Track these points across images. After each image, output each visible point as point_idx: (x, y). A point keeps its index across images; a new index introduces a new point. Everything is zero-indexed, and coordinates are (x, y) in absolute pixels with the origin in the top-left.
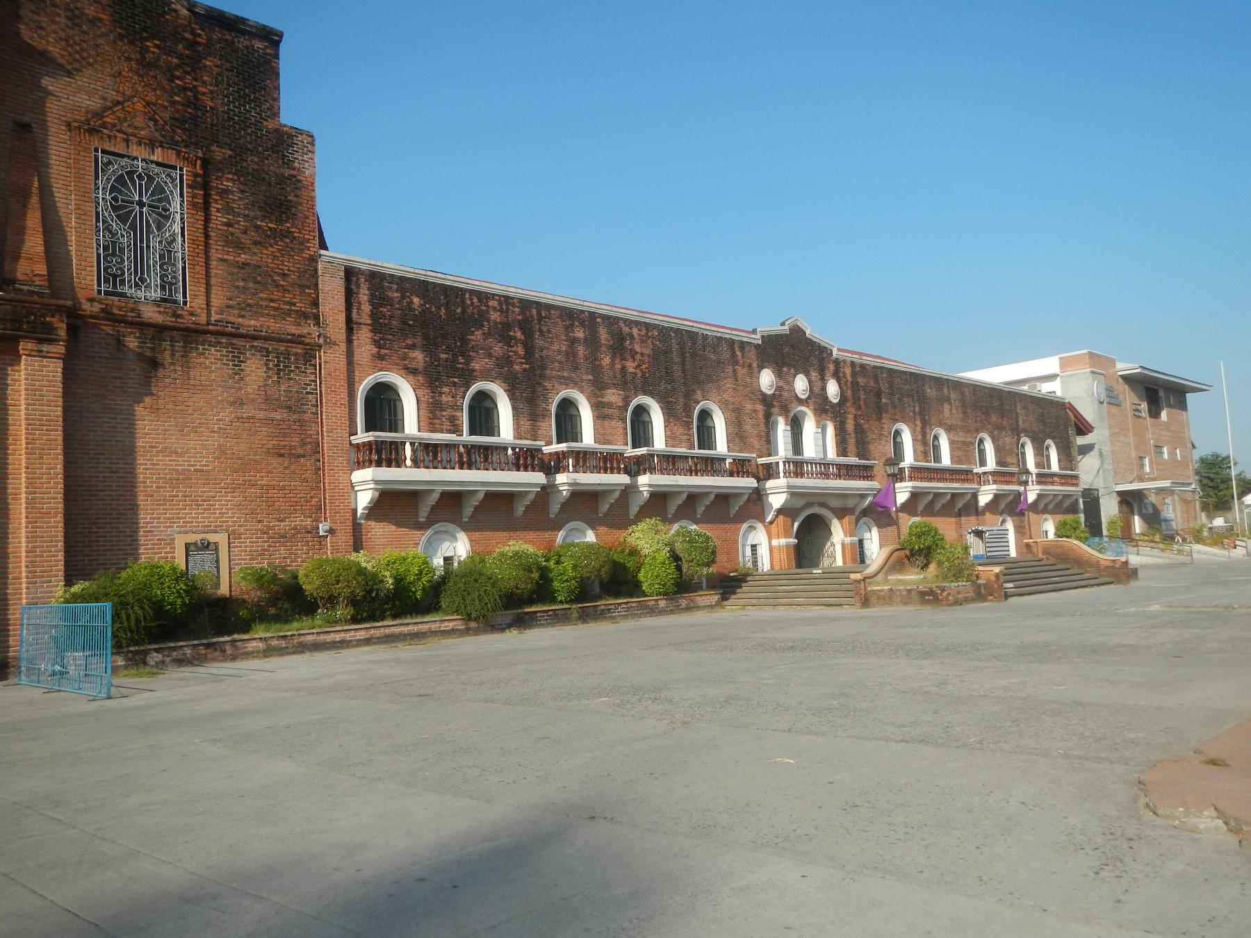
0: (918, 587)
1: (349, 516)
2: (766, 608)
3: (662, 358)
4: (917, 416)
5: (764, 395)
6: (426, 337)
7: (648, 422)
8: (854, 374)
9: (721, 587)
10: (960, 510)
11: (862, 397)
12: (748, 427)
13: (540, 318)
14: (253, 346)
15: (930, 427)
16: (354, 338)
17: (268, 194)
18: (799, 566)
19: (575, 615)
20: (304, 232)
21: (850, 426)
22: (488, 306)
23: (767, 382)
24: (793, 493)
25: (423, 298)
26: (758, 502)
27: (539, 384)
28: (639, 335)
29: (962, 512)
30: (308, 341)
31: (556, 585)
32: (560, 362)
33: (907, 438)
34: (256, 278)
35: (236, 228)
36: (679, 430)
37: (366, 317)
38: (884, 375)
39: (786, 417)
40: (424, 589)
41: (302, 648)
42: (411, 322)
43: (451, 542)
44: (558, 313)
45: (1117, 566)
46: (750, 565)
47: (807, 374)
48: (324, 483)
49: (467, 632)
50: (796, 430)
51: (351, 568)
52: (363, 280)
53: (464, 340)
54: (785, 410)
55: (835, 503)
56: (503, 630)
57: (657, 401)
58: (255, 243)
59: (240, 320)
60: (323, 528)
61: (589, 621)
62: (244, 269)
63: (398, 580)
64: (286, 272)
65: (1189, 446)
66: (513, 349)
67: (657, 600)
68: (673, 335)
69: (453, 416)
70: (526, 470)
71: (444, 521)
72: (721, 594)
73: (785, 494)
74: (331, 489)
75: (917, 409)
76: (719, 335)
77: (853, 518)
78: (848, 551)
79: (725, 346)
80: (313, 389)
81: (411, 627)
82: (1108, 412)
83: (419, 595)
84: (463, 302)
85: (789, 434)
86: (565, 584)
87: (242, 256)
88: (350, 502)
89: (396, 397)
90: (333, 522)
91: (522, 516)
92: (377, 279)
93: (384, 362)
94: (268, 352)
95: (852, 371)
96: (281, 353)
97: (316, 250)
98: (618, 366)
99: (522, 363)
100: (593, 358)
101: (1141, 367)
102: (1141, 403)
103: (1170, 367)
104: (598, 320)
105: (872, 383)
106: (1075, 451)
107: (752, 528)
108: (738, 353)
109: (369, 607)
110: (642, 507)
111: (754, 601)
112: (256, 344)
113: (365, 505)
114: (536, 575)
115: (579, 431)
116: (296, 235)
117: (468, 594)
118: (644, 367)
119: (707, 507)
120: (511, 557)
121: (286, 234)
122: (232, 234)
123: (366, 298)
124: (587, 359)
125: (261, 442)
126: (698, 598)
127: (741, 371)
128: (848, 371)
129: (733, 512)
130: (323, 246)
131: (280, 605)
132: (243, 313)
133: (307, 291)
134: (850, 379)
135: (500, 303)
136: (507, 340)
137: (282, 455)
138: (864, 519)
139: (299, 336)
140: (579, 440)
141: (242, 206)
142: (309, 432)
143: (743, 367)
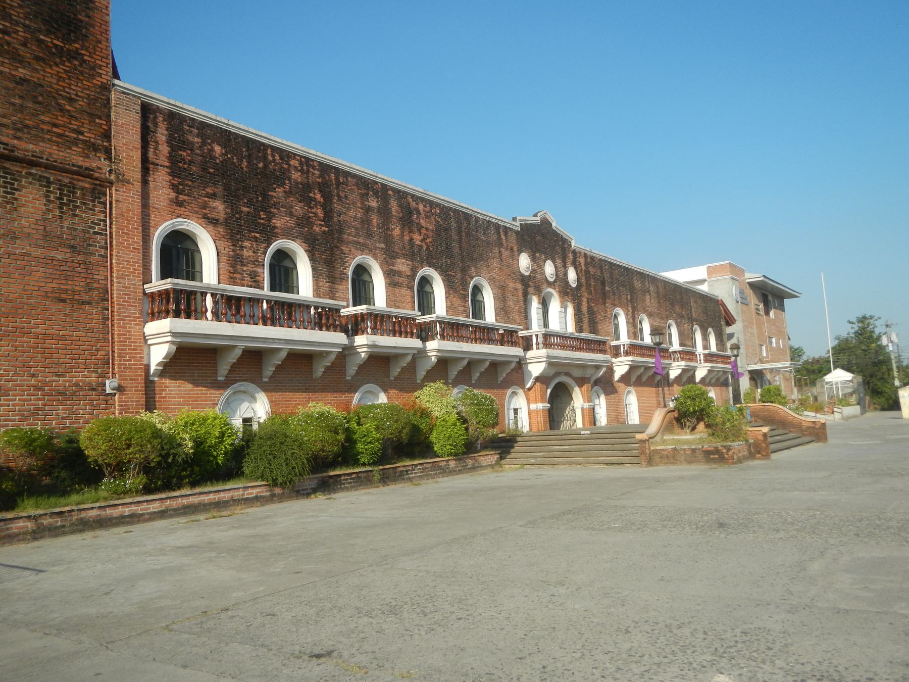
0: (703, 447)
1: (141, 372)
2: (545, 467)
3: (443, 234)
4: (629, 303)
5: (522, 275)
6: (227, 188)
7: (430, 293)
8: (586, 264)
9: (500, 447)
10: (658, 382)
12: (510, 303)
13: (338, 184)
14: (30, 174)
16: (150, 179)
17: (54, 7)
19: (377, 477)
20: (95, 57)
21: (584, 308)
22: (289, 165)
23: (525, 265)
24: (551, 363)
25: (225, 148)
27: (336, 247)
28: (424, 210)
30: (97, 175)
31: (360, 446)
32: (356, 229)
33: (622, 321)
34: (36, 97)
35: (13, 38)
36: (458, 302)
37: (164, 159)
38: (607, 267)
39: (539, 296)
40: (226, 453)
41: (85, 526)
42: (211, 171)
43: (250, 402)
44: (354, 180)
45: (817, 427)
47: (554, 262)
48: (112, 334)
49: (272, 499)
51: (145, 430)
52: (161, 119)
53: (265, 196)
54: (538, 290)
55: (577, 373)
56: (308, 495)
57: (439, 273)
58: (38, 59)
59: (16, 141)
60: (110, 385)
61: (389, 483)
62: (22, 85)
63: (199, 443)
64: (73, 96)
66: (313, 210)
67: (447, 461)
68: (452, 214)
69: (255, 272)
70: (328, 330)
71: (244, 381)
72: (499, 454)
74: (120, 342)
75: (629, 297)
77: (590, 385)
78: (587, 414)
79: (492, 230)
80: (102, 229)
81: (211, 496)
82: (742, 309)
83: (220, 459)
84: (265, 157)
86: (369, 446)
87: (20, 70)
88: (142, 357)
89: (192, 247)
90: (122, 378)
91: (321, 377)
92: (175, 120)
93: (182, 209)
94: (49, 183)
96: (64, 186)
97: (109, 78)
98: (407, 238)
99: (321, 225)
100: (385, 227)
101: (764, 276)
102: (760, 304)
103: (782, 278)
104: (390, 192)
106: (725, 337)
107: (514, 393)
108: (503, 237)
109: (163, 474)
110: (429, 372)
111: (533, 461)
112: (34, 171)
113: (160, 360)
114: (341, 437)
115: (372, 296)
116: (86, 58)
117: (274, 458)
118: (428, 240)
119: (482, 373)
120: (317, 418)
121: (74, 55)
122: (8, 43)
123: (164, 138)
124: (380, 228)
125: (36, 284)
126: (481, 458)
127: (506, 253)
128: (582, 261)
129: (501, 379)
130: (116, 76)
131: (57, 474)
132: (19, 134)
133: (97, 121)
134: (584, 269)
135: (301, 163)
136: (308, 201)
137: (63, 301)
138: (596, 388)
139: (87, 169)
140: (372, 303)
141: (22, 15)
142: (95, 277)
143: (507, 250)
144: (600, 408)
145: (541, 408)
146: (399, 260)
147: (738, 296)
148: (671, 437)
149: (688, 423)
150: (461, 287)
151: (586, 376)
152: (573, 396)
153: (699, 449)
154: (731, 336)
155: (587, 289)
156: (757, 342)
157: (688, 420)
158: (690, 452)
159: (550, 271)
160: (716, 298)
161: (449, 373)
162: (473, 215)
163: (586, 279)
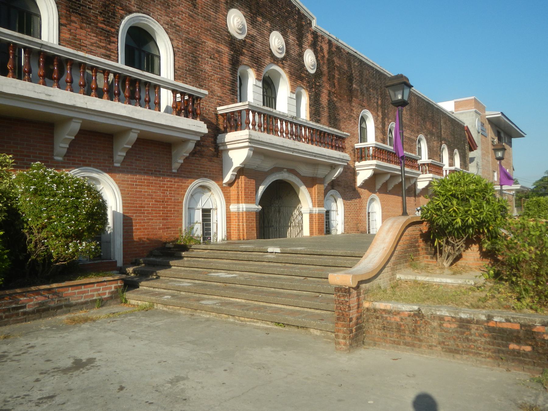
0: (490, 318)
4: (379, 108)
8: (330, 52)
11: (337, 76)
21: (324, 100)
26: (215, 159)
33: (371, 125)
38: (356, 64)
39: (258, 71)
46: (198, 230)
50: (269, 94)
54: (257, 64)
55: (305, 171)
65: (512, 168)
73: (247, 149)
75: (379, 102)
77: (323, 187)
78: (316, 220)
82: (481, 140)
85: (261, 91)
95: (329, 49)
101: (502, 113)
105: (346, 67)
107: (205, 188)
119: (129, 153)
126: (70, 291)
128: (326, 47)
134: (327, 56)
138: (332, 192)
144: (338, 214)
145: (245, 209)
147: (480, 128)
148: (411, 277)
149: (447, 249)
150: (100, 18)
152: (300, 197)
153: (478, 322)
154: (472, 160)
155: (329, 80)
156: (491, 169)
157: (448, 243)
158: (454, 326)
159: (276, 44)
160: (462, 124)
163: (328, 68)
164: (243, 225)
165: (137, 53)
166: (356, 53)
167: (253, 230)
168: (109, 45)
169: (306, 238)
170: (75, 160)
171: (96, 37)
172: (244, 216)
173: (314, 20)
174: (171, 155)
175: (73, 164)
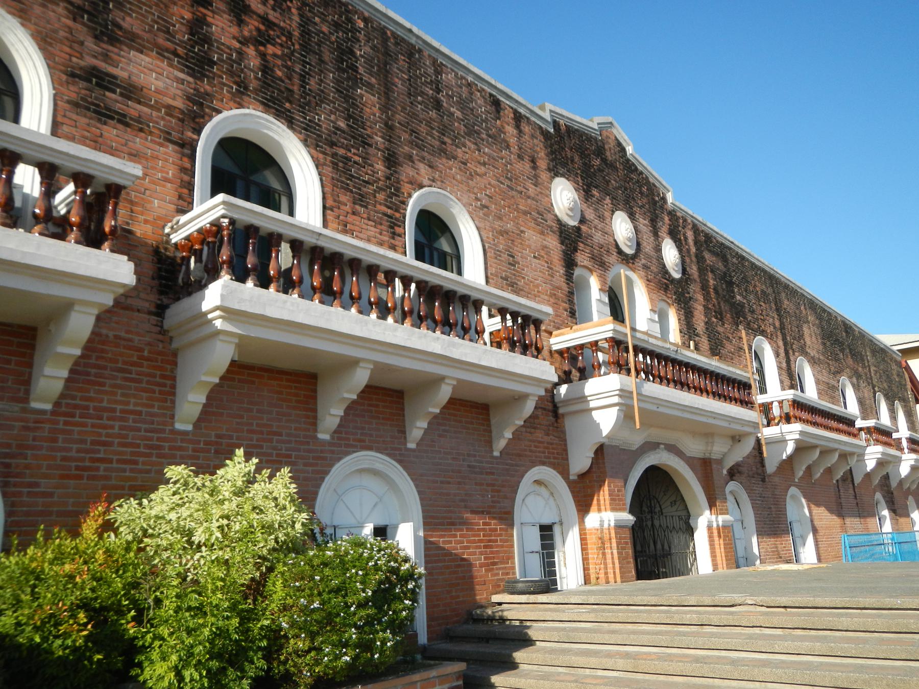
5: (559, 221)
10: (837, 481)
15: (794, 354)
18: (644, 573)
29: (840, 483)
47: (632, 216)
54: (601, 265)
55: (695, 447)
76: (470, 79)
95: (695, 237)
105: (720, 265)
118: (270, 49)
119: (436, 422)
128: (690, 234)
129: (500, 444)
134: (693, 250)
145: (612, 524)
146: (144, 59)
151: (714, 457)
161: (320, 413)
162: (426, 53)
164: (612, 553)
165: (427, 251)
166: (732, 243)
167: (628, 563)
168: (393, 238)
169: (706, 577)
170: (348, 439)
171: (375, 227)
172: (613, 535)
173: (670, 193)
174: (489, 426)
175: (347, 446)
